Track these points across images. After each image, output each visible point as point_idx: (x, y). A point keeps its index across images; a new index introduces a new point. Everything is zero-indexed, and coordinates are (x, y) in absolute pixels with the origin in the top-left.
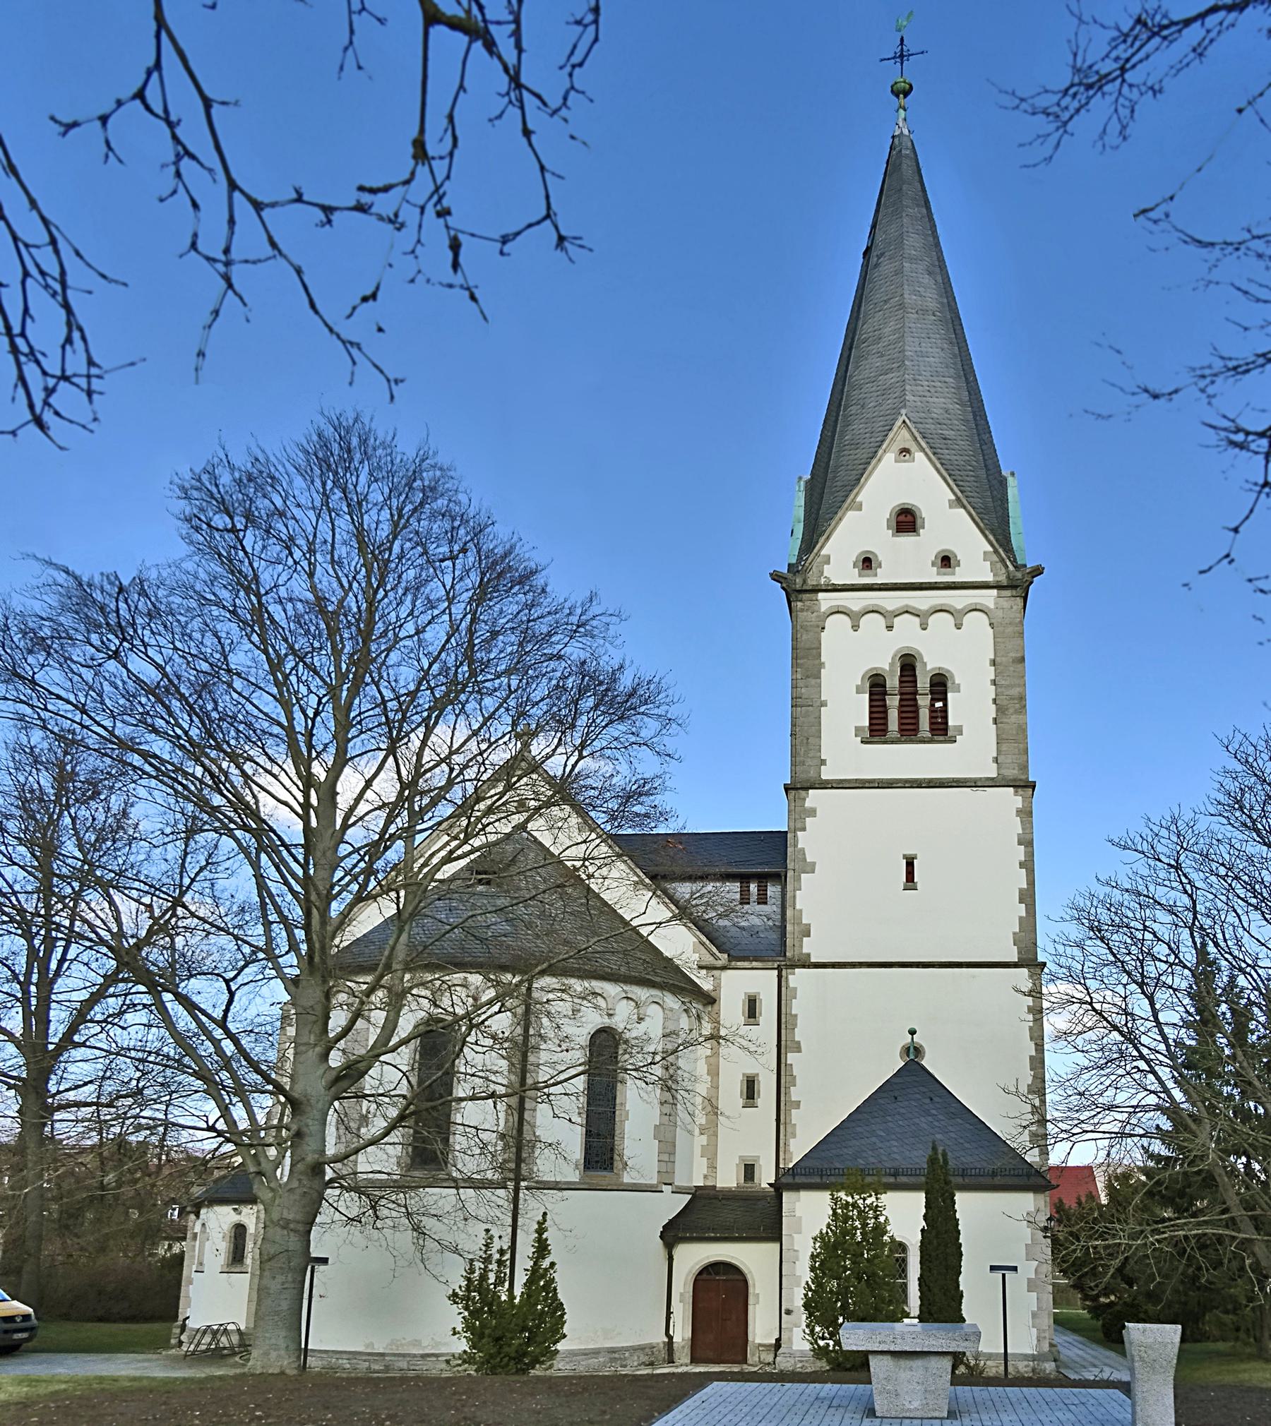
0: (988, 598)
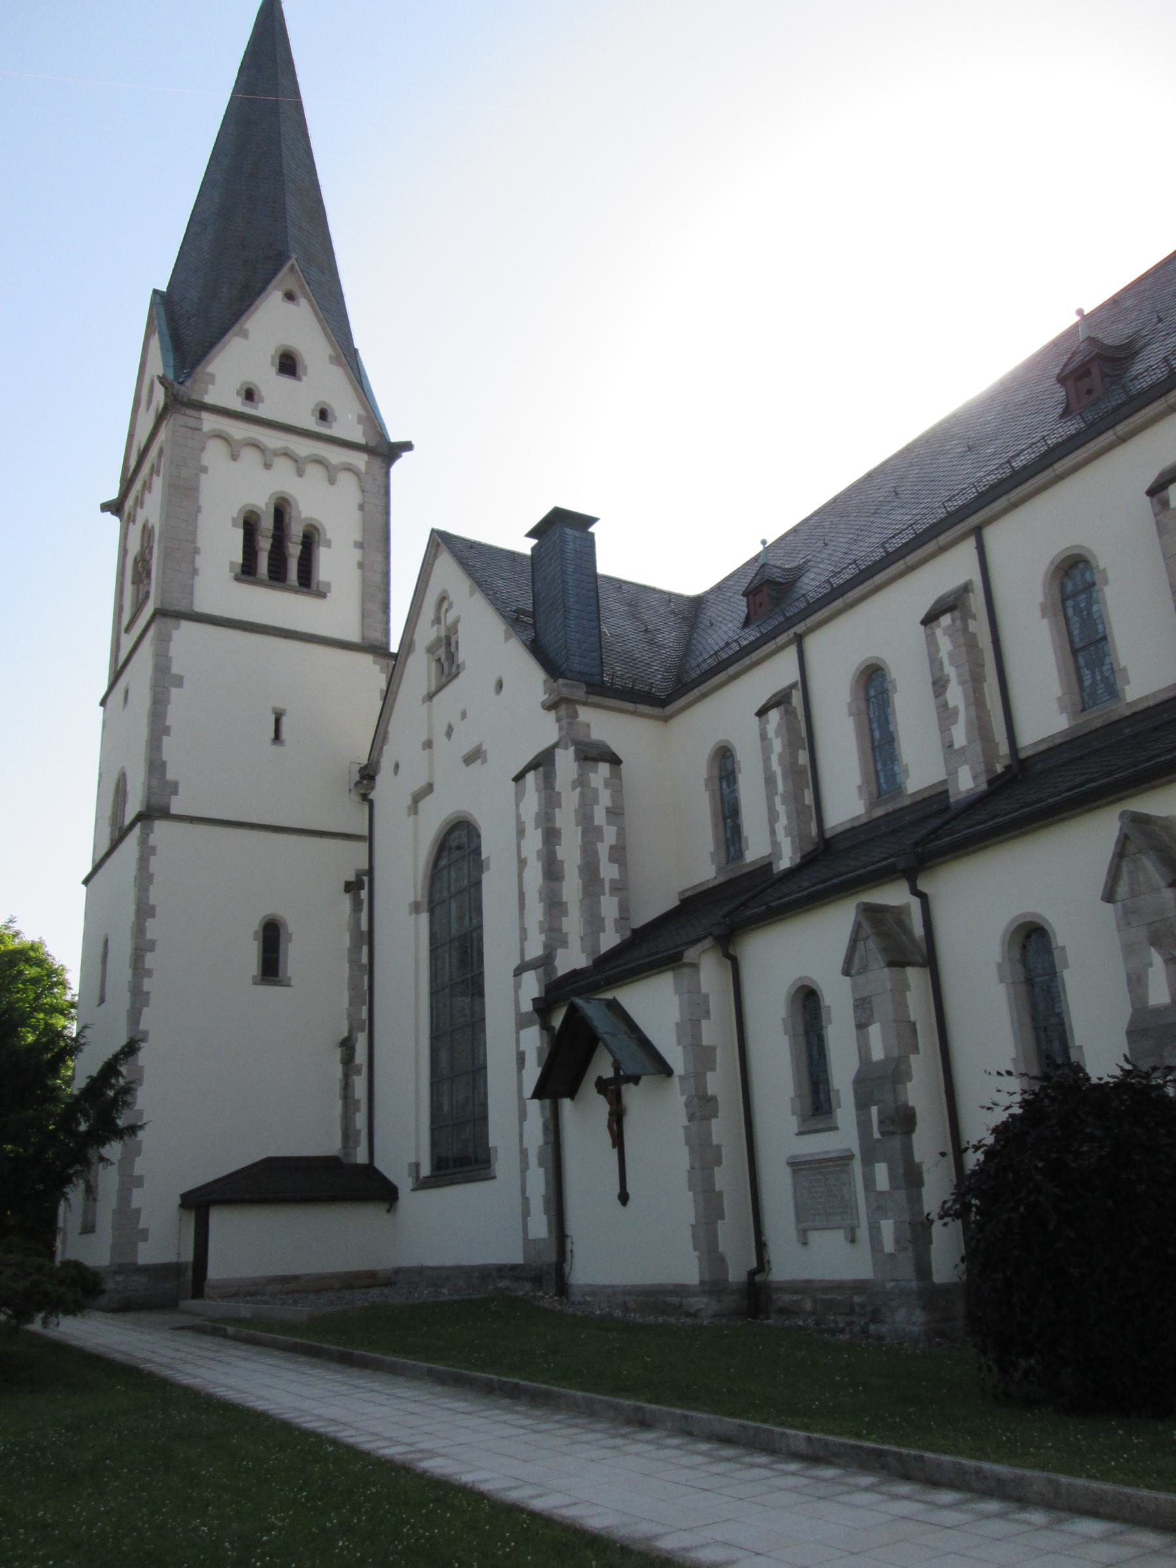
0: (360, 460)
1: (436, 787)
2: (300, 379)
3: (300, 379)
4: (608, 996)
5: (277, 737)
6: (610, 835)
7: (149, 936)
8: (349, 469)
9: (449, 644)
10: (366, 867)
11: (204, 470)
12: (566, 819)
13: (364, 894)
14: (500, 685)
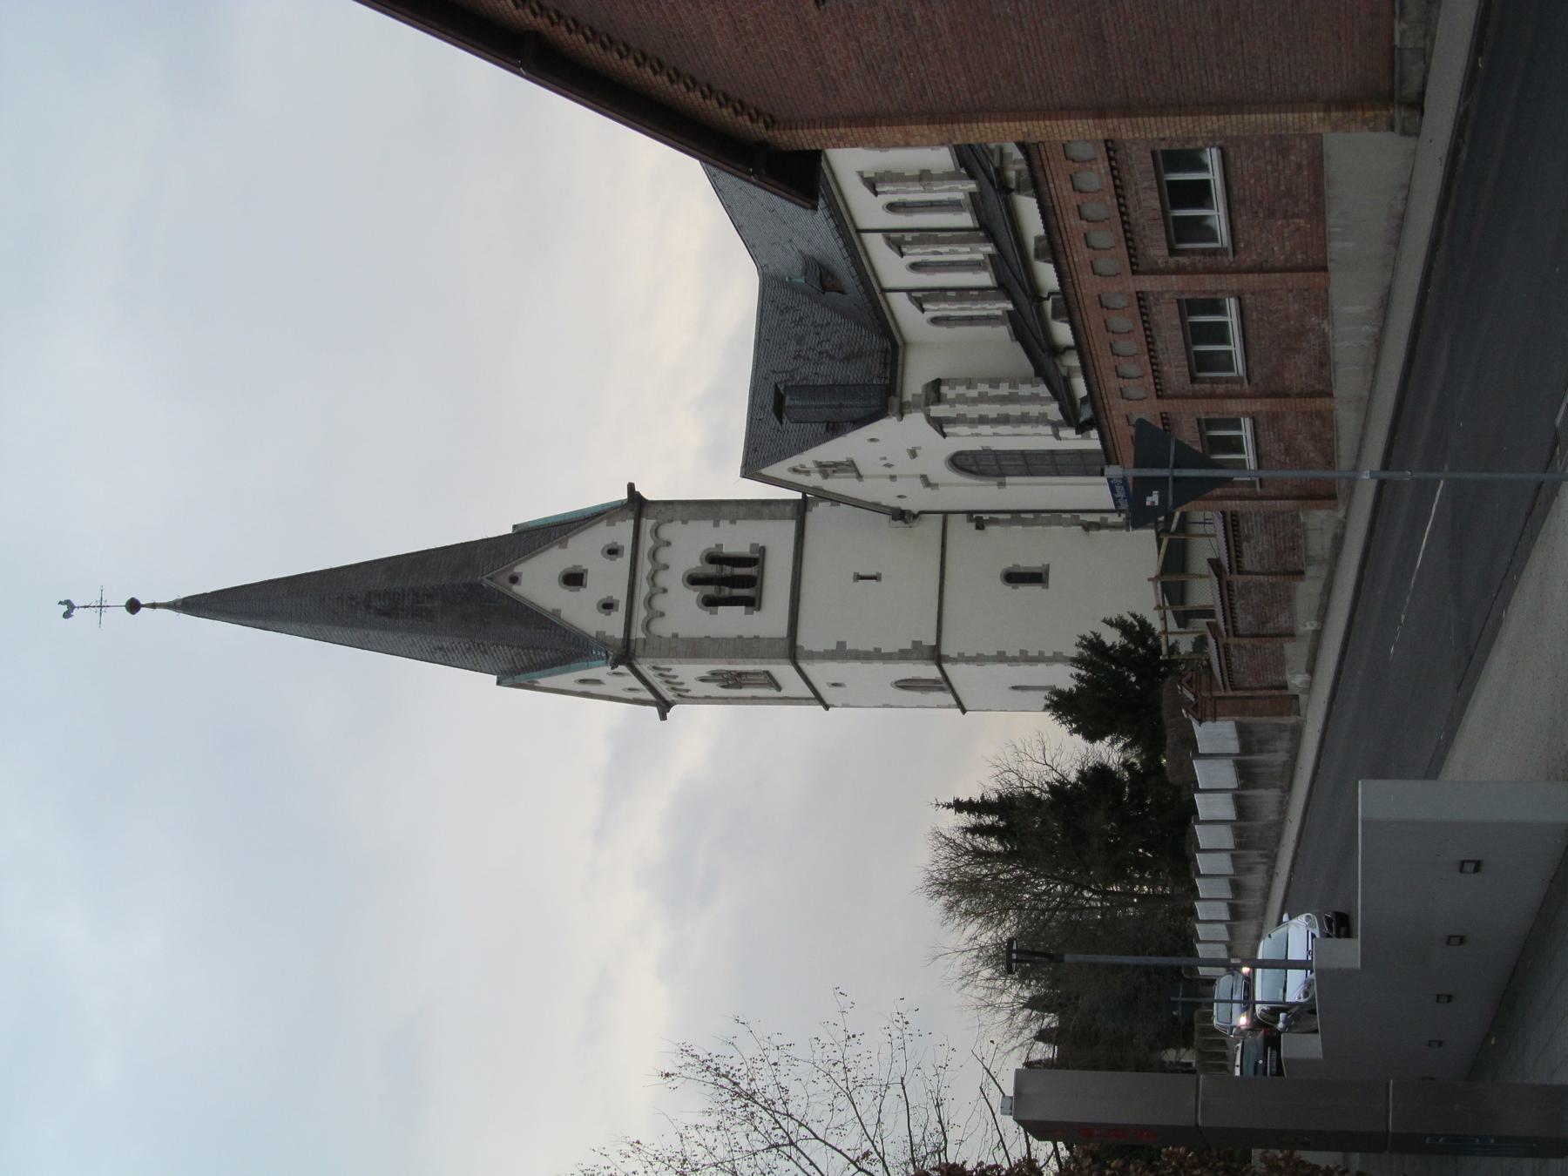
0: (648, 524)
1: (924, 473)
2: (586, 571)
3: (586, 571)
4: (1079, 402)
5: (875, 578)
6: (983, 388)
7: (1017, 654)
8: (655, 532)
9: (826, 466)
10: (965, 515)
11: (675, 636)
12: (973, 411)
13: (986, 517)
14: (873, 440)
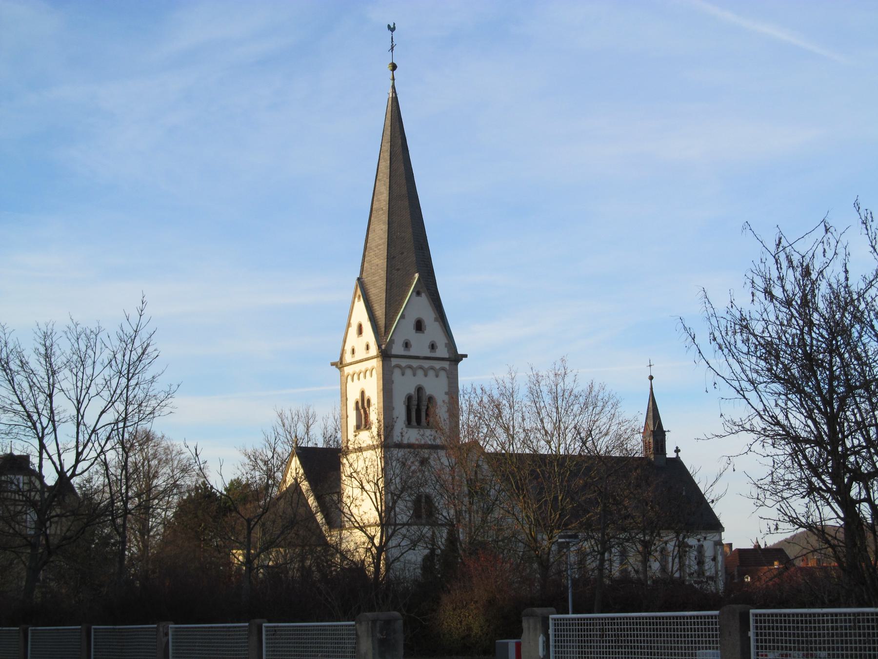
0: (446, 365)
2: (423, 333)
8: (443, 369)
